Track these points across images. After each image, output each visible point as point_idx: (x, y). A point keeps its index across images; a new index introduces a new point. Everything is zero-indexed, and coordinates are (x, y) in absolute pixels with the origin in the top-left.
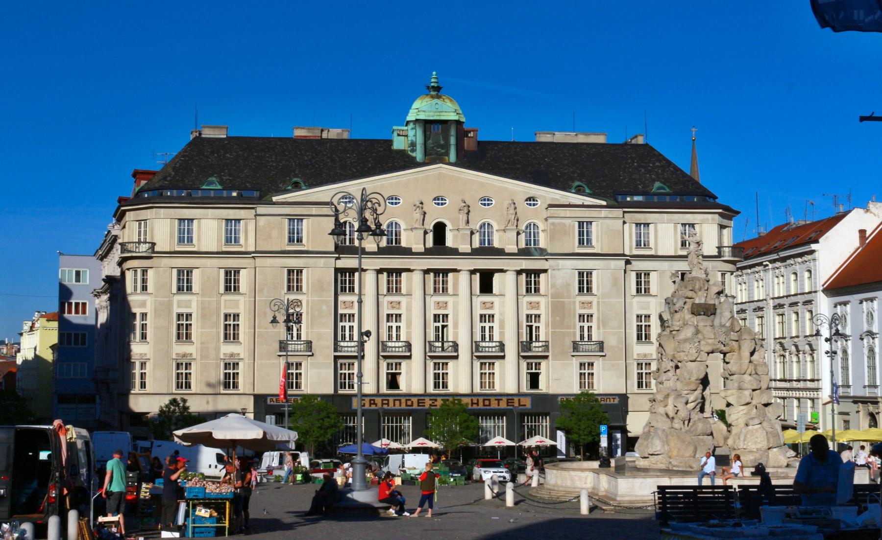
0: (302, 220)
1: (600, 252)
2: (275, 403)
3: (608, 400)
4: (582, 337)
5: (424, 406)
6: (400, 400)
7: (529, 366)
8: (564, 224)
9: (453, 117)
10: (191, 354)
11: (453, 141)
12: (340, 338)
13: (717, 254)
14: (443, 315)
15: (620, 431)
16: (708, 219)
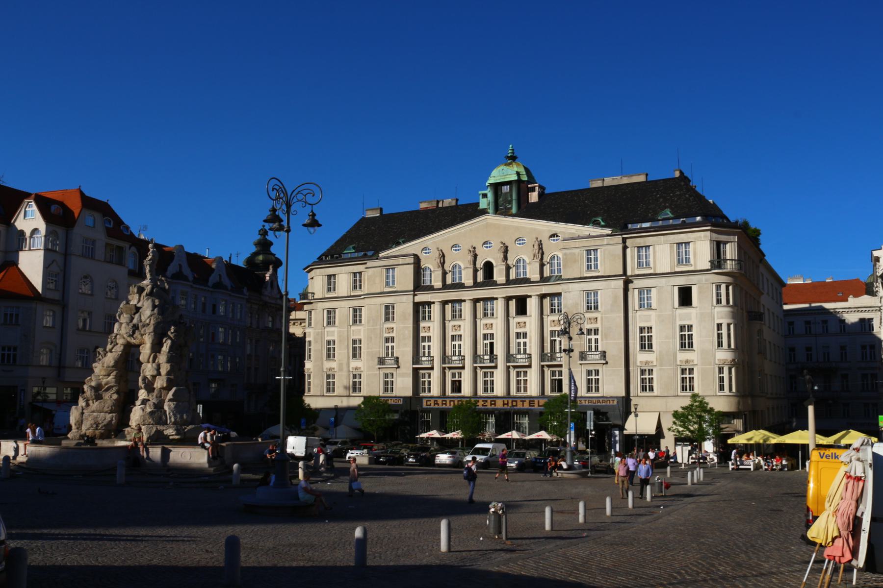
0: (394, 268)
1: (603, 275)
3: (608, 402)
4: (590, 348)
6: (454, 401)
7: (553, 373)
8: (574, 254)
9: (515, 177)
10: (334, 369)
11: (514, 196)
12: (421, 354)
13: (710, 268)
14: (491, 334)
15: (618, 429)
16: (700, 237)
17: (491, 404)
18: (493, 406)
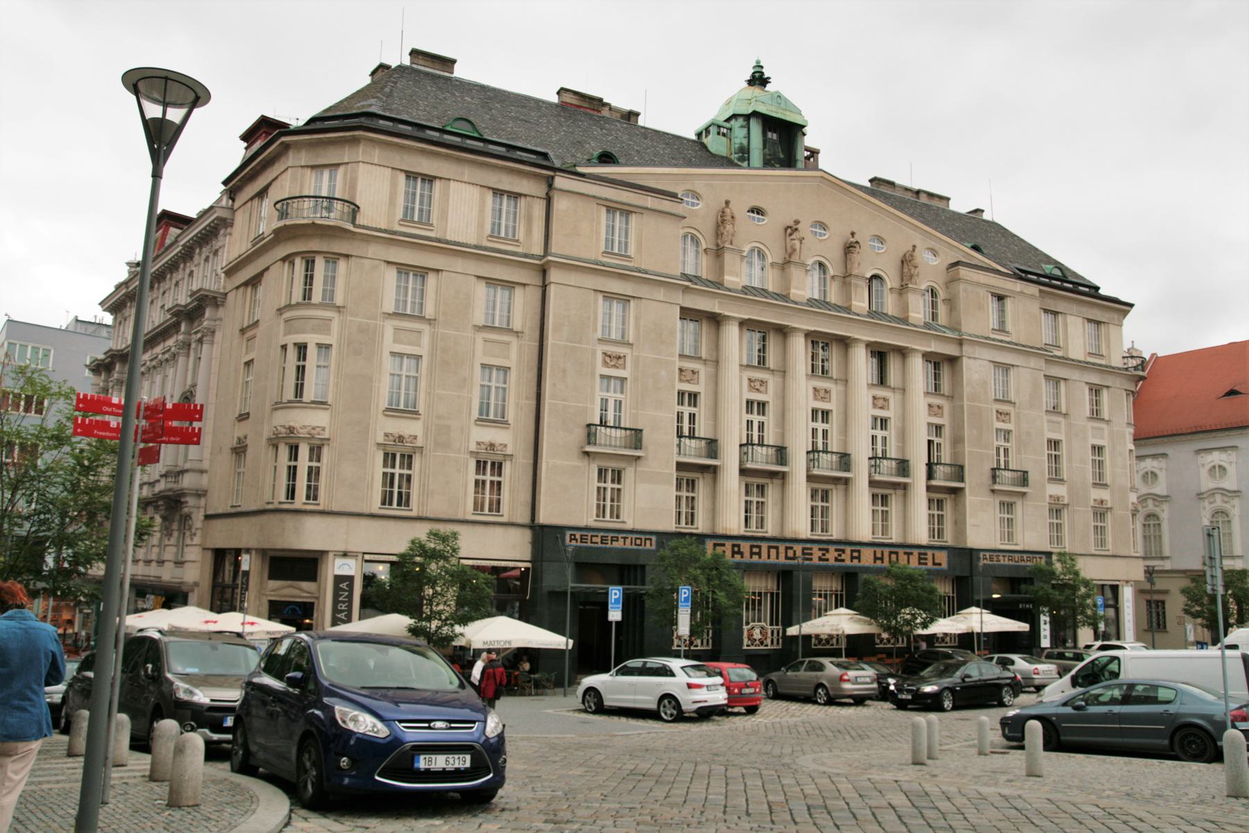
2: (579, 544)
5: (811, 559)
6: (777, 548)
17: (852, 558)
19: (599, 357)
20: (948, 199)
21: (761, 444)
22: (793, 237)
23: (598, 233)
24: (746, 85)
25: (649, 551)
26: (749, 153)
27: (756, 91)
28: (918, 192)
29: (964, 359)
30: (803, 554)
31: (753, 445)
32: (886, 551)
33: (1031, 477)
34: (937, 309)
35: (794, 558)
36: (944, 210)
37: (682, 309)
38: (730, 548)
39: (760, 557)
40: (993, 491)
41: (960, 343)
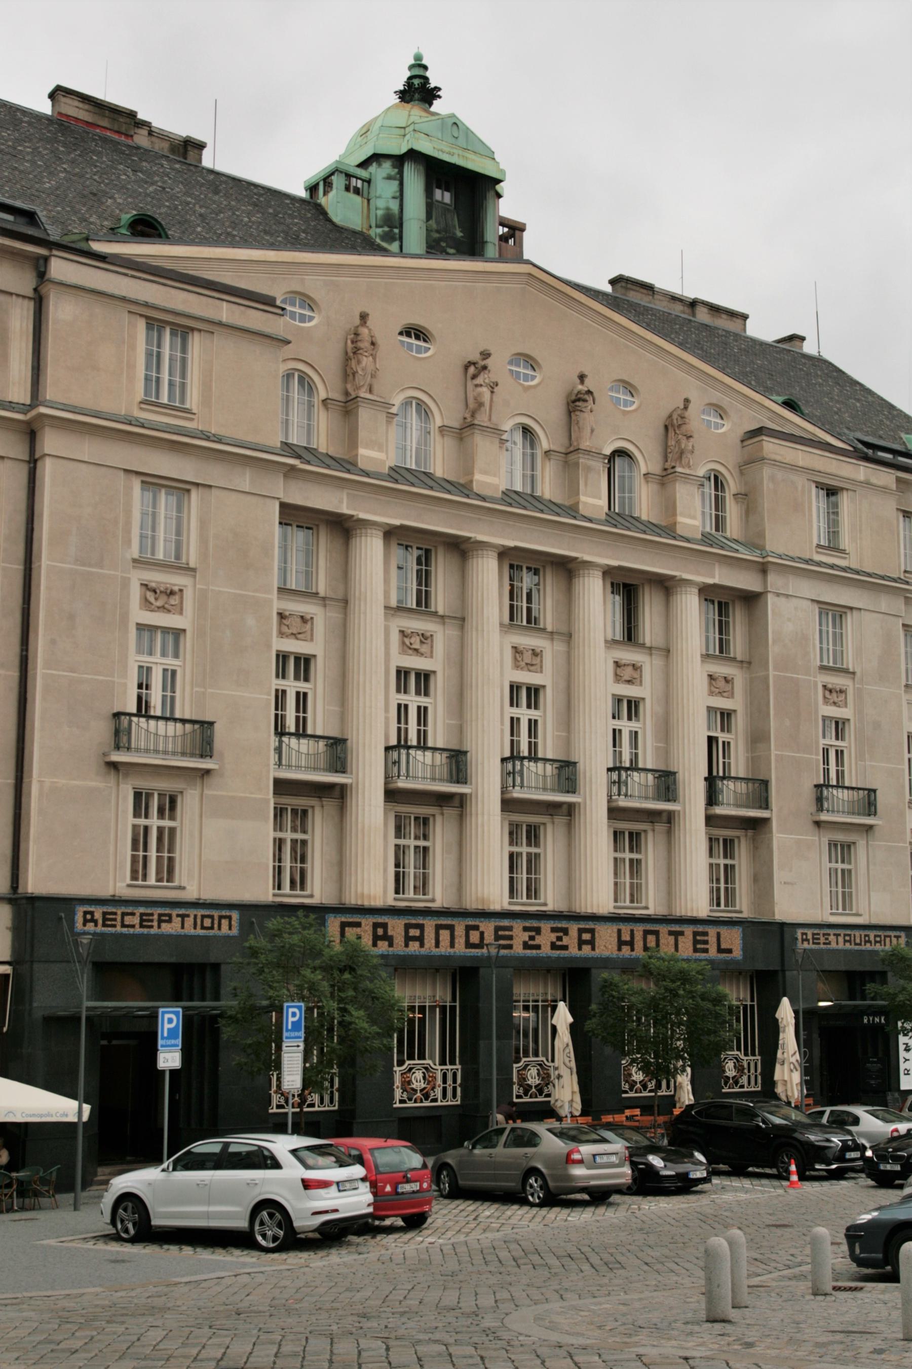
2: (100, 929)
5: (510, 947)
6: (451, 928)
17: (581, 943)
18: (586, 949)
19: (136, 592)
20: (745, 317)
21: (422, 746)
22: (479, 380)
23: (131, 366)
24: (395, 100)
25: (227, 937)
26: (401, 226)
27: (415, 112)
28: (693, 304)
29: (771, 599)
30: (497, 938)
31: (409, 748)
32: (639, 929)
33: (882, 799)
34: (723, 510)
35: (480, 945)
36: (736, 335)
37: (283, 506)
38: (370, 932)
39: (422, 945)
40: (818, 824)
41: (763, 569)
